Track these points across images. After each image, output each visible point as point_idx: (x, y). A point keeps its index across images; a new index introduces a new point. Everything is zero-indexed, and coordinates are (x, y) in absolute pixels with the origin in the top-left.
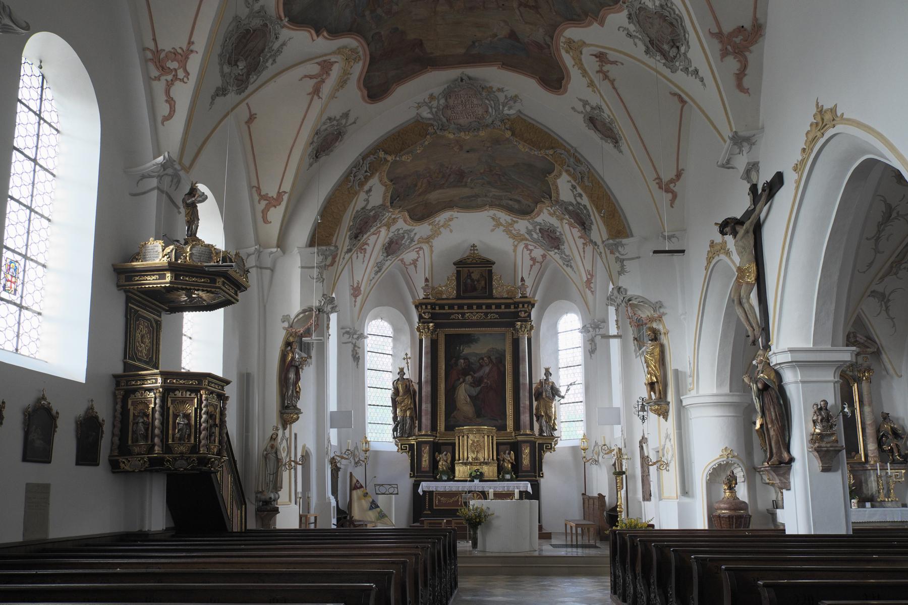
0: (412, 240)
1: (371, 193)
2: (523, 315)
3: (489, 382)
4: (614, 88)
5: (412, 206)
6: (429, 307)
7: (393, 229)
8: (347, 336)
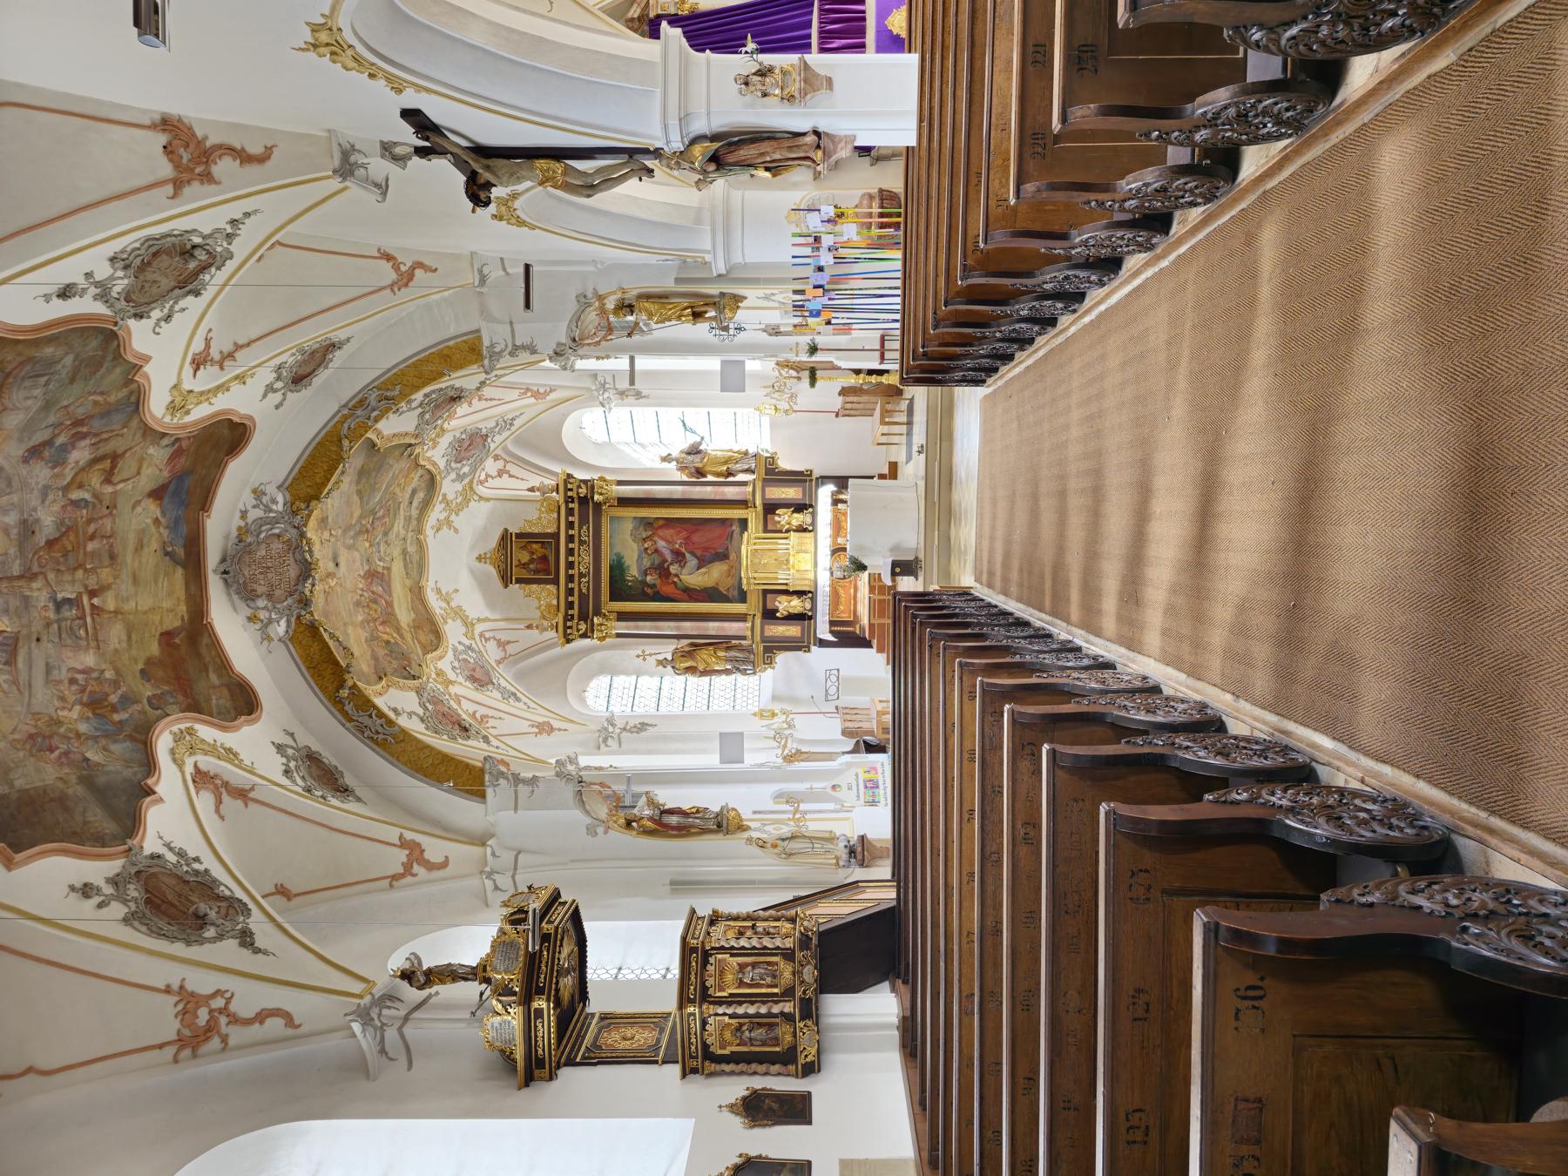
0: (470, 648)
1: (399, 708)
2: (583, 491)
4: (248, 345)
5: (419, 649)
6: (569, 624)
7: (451, 676)
8: (610, 742)
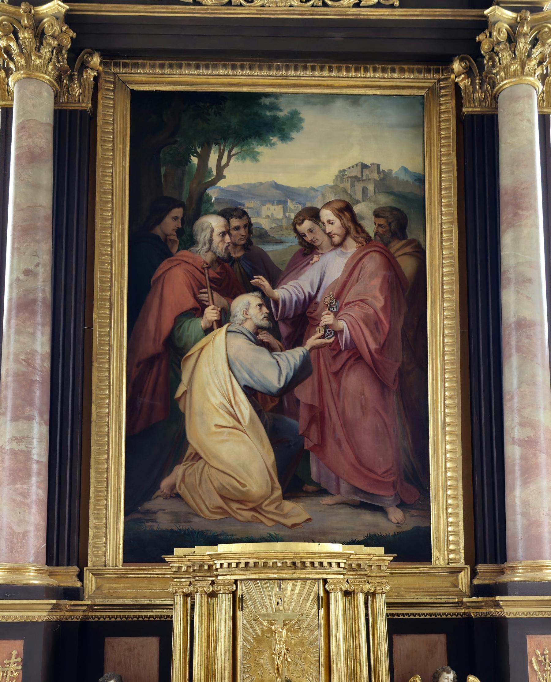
3: (342, 325)
